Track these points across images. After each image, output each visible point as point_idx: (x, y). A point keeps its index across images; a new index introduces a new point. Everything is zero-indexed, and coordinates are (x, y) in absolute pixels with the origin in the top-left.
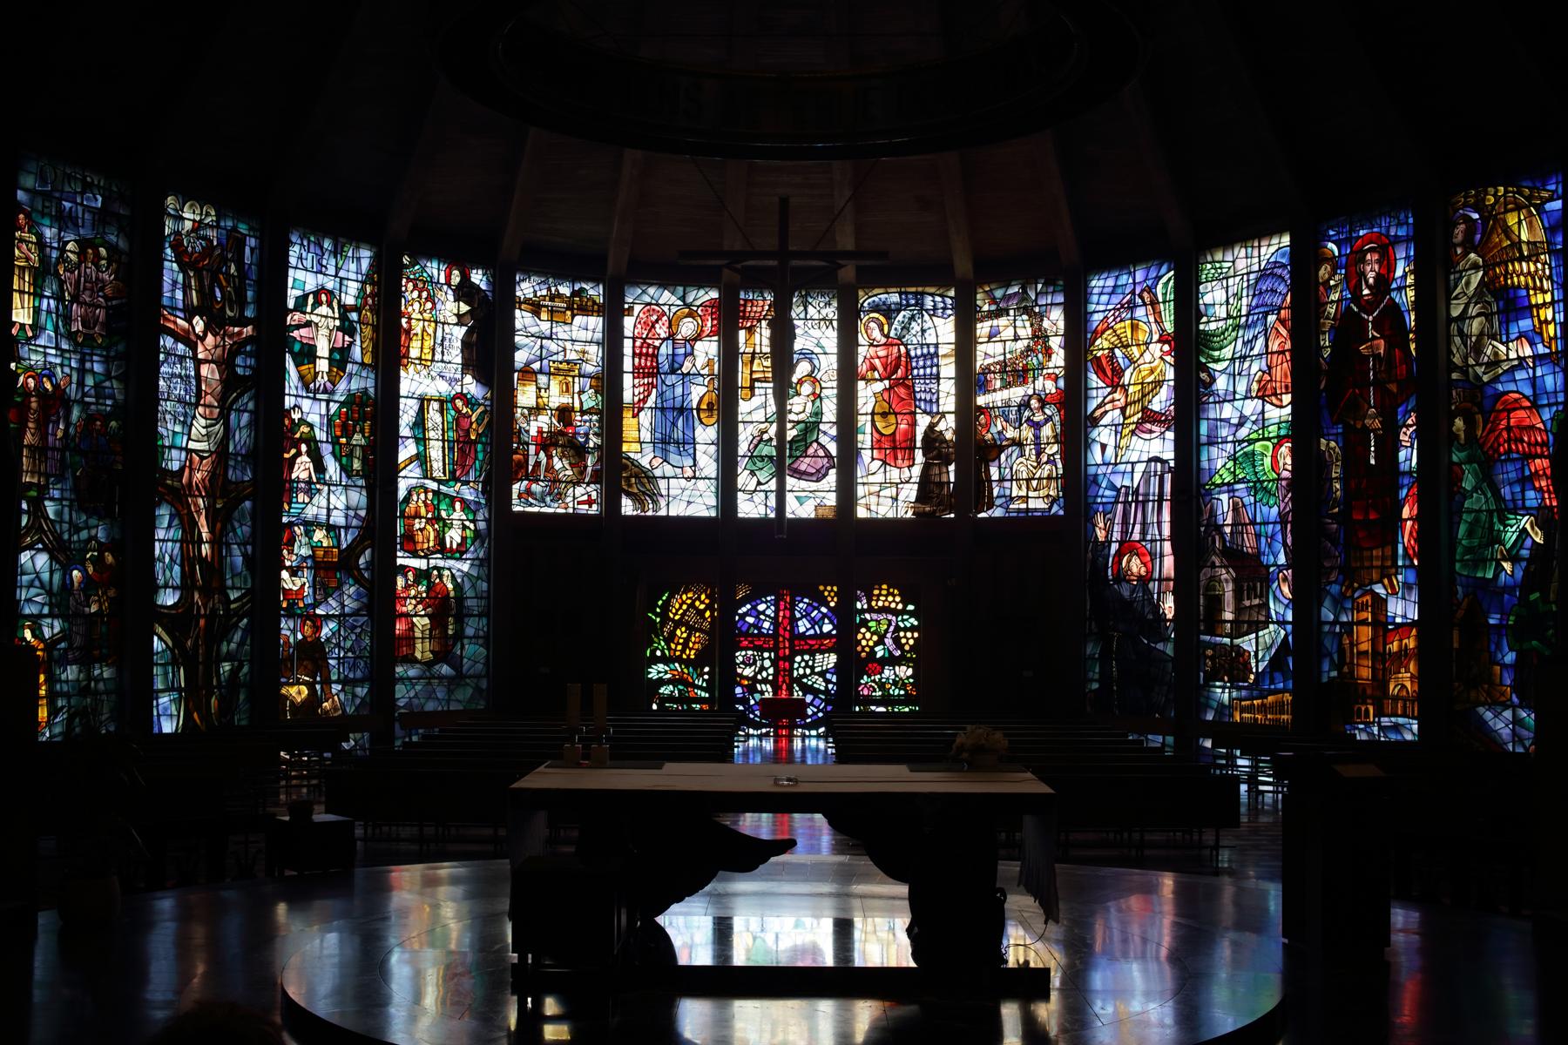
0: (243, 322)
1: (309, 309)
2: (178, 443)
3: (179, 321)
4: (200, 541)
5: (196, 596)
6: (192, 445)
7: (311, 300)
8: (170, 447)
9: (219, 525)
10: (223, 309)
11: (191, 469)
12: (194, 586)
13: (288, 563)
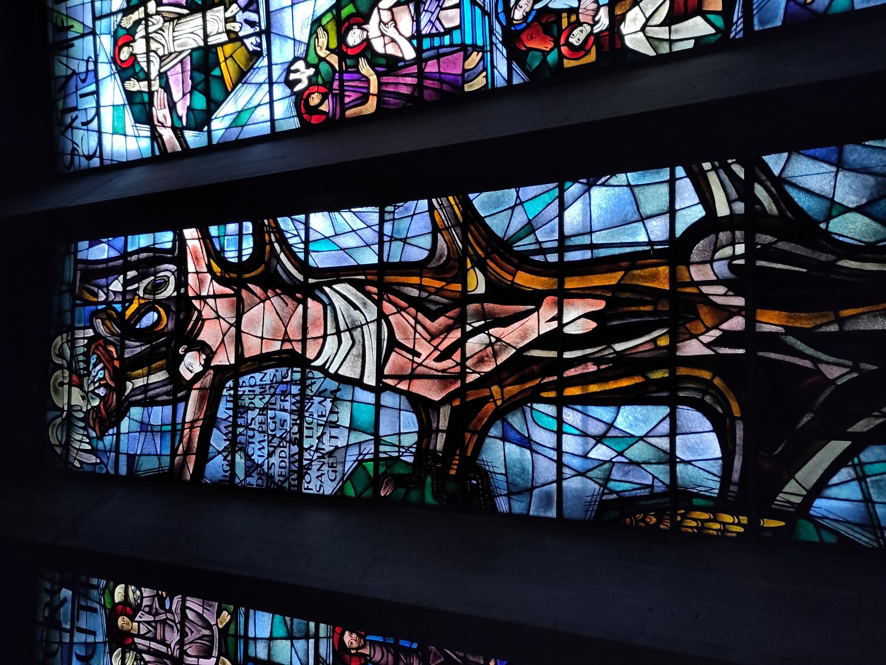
0: (178, 255)
1: (143, 86)
2: (366, 416)
3: (188, 418)
4: (556, 339)
5: (692, 348)
6: (370, 379)
7: (134, 86)
8: (378, 440)
9: (524, 280)
10: (165, 304)
11: (412, 377)
12: (669, 358)
13: (604, 19)
